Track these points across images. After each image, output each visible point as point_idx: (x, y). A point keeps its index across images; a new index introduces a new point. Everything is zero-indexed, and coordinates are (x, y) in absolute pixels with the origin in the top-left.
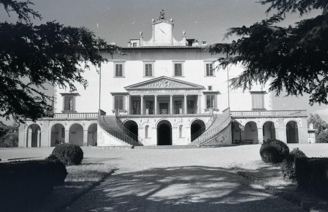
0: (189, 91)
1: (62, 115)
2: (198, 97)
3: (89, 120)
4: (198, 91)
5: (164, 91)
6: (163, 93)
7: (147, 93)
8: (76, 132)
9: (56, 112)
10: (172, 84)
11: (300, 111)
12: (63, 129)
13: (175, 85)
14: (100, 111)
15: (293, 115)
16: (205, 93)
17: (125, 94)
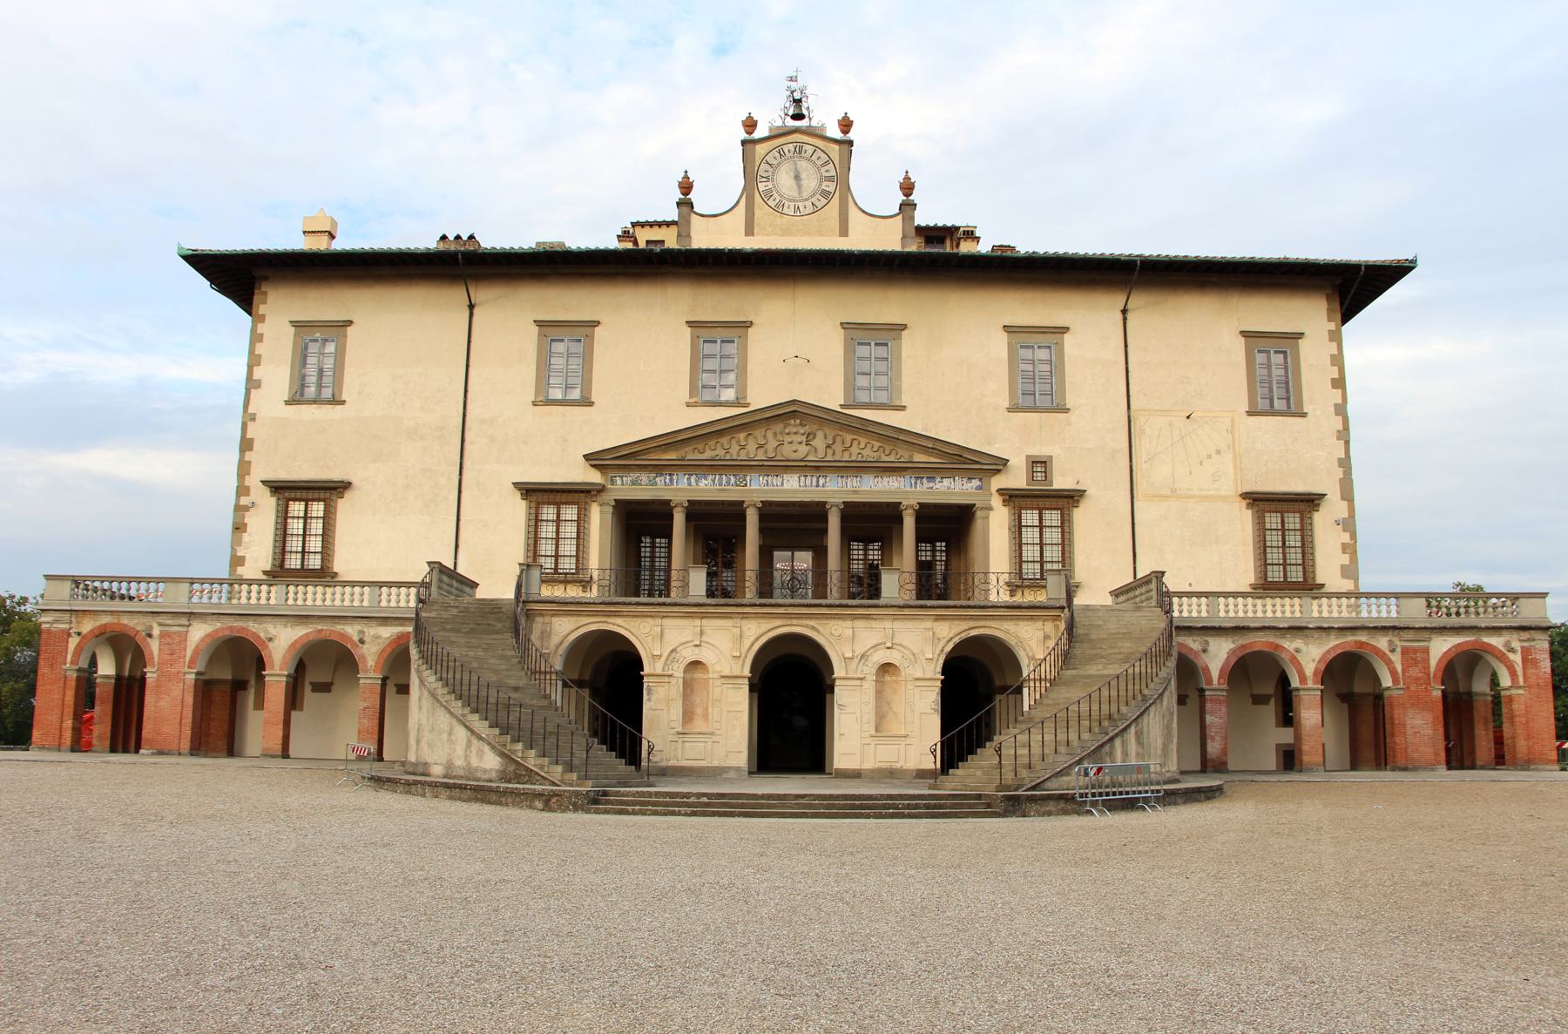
0: (931, 485)
1: (264, 588)
2: (979, 514)
3: (385, 621)
4: (975, 483)
5: (796, 477)
6: (792, 487)
7: (708, 488)
8: (332, 684)
9: (242, 576)
10: (838, 447)
11: (1517, 598)
12: (260, 664)
13: (855, 450)
14: (435, 573)
15: (1449, 619)
16: (1012, 497)
17: (589, 492)
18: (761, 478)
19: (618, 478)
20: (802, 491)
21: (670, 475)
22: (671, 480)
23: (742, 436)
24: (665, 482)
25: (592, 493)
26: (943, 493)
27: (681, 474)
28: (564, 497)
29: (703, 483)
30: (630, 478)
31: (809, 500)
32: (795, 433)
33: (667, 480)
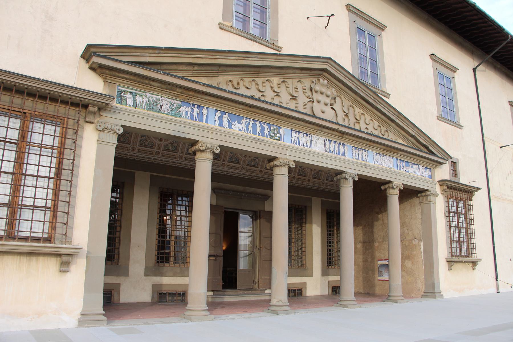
0: (408, 169)
2: (432, 198)
18: (293, 134)
19: (128, 95)
20: (328, 156)
21: (199, 106)
22: (199, 114)
23: (275, 81)
24: (192, 115)
25: (91, 108)
26: (413, 178)
27: (212, 110)
28: (40, 106)
29: (237, 127)
30: (146, 100)
31: (332, 167)
32: (322, 93)
33: (195, 114)
